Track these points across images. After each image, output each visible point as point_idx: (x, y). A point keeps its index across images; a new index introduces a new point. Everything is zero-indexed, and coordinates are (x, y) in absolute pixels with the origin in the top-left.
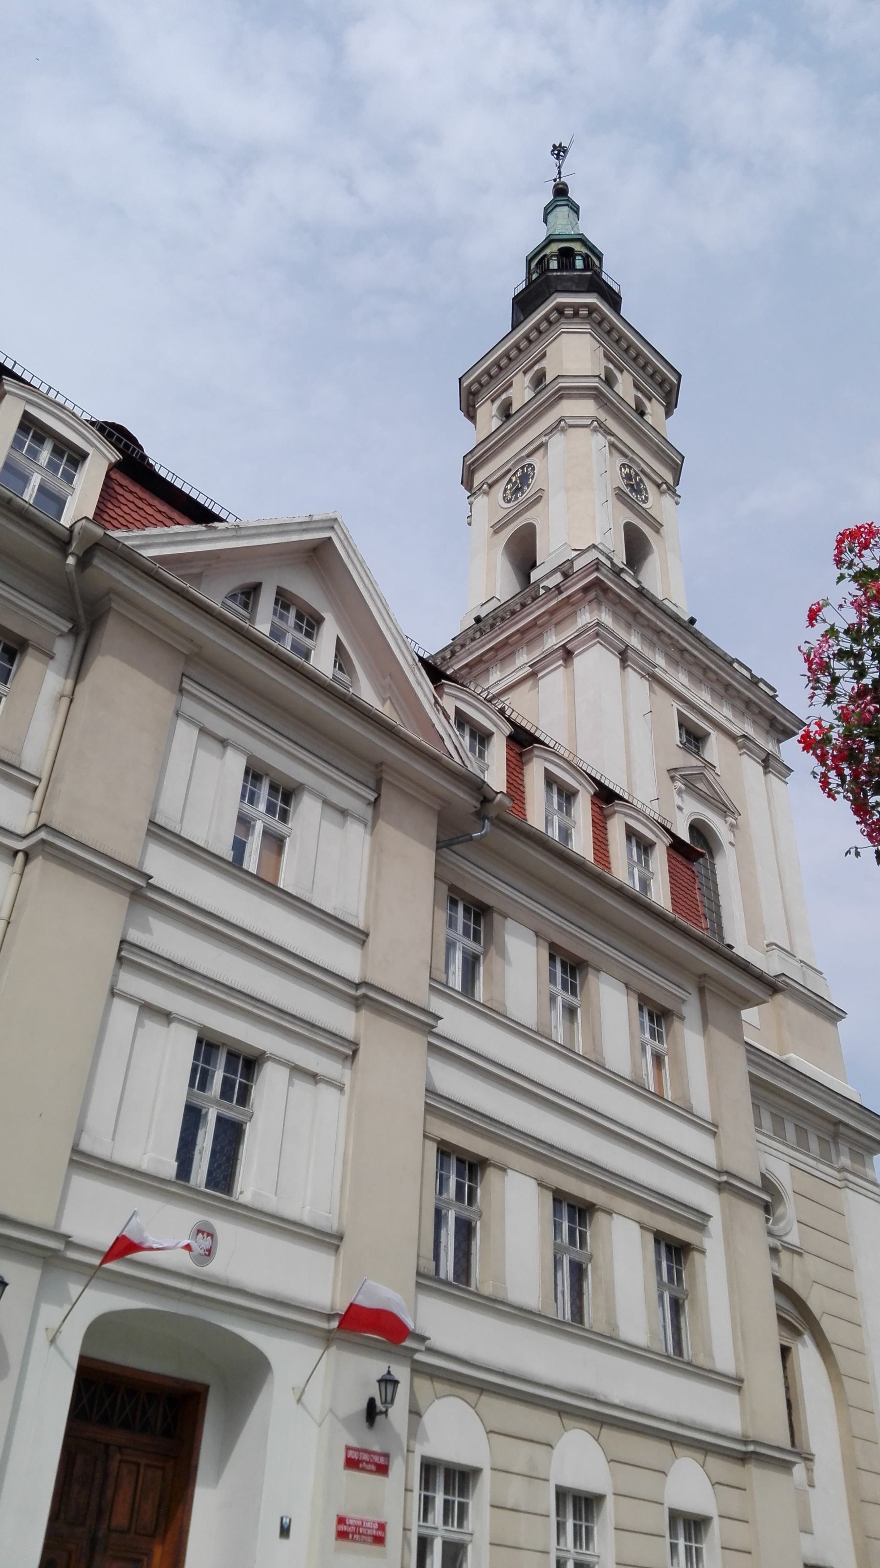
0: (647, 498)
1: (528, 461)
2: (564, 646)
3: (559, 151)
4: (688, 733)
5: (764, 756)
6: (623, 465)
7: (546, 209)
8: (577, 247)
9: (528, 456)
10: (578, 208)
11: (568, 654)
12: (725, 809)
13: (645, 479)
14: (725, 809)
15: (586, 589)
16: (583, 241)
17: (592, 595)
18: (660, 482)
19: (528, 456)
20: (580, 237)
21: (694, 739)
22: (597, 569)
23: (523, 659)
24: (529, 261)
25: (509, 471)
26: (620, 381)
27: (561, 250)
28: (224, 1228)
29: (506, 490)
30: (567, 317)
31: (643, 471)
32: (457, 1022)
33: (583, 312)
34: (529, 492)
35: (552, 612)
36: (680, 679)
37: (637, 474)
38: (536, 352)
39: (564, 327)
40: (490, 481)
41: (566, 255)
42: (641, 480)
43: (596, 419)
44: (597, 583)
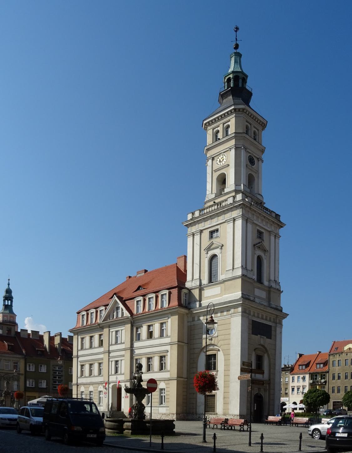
0: (254, 164)
3: (237, 29)
6: (249, 156)
12: (265, 251)
14: (265, 251)
21: (260, 234)
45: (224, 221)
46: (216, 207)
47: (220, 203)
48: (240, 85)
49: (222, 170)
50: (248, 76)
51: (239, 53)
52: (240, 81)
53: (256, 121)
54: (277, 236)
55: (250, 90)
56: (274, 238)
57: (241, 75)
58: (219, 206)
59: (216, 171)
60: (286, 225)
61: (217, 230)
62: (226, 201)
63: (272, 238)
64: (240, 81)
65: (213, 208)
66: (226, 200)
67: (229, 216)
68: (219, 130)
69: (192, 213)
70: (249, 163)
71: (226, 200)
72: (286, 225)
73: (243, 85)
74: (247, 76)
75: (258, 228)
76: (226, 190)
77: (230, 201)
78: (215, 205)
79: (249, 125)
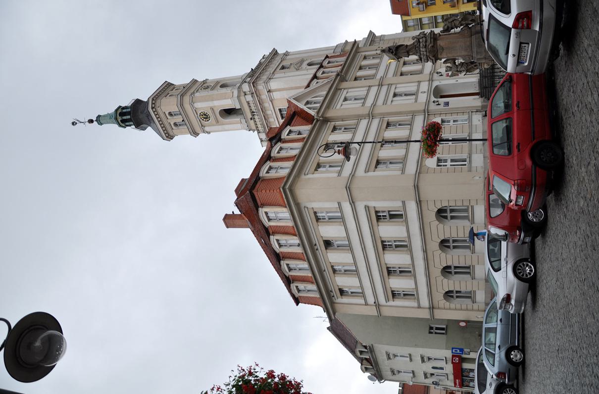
1: (199, 114)
2: (268, 92)
7: (99, 124)
8: (118, 112)
9: (197, 114)
10: (99, 115)
11: (269, 91)
12: (302, 61)
15: (254, 86)
16: (116, 110)
19: (197, 114)
21: (283, 68)
23: (267, 104)
24: (120, 126)
27: (120, 116)
28: (420, 91)
29: (205, 121)
30: (155, 106)
32: (381, 73)
33: (154, 102)
34: (210, 113)
35: (257, 96)
36: (271, 70)
38: (162, 115)
40: (201, 126)
43: (191, 94)
44: (253, 83)
45: (270, 103)
46: (256, 117)
48: (129, 110)
49: (216, 113)
51: (97, 117)
52: (124, 111)
54: (287, 54)
56: (288, 56)
57: (120, 111)
59: (217, 122)
61: (280, 110)
62: (249, 103)
63: (288, 57)
64: (124, 111)
65: (257, 120)
66: (248, 103)
67: (264, 96)
70: (209, 89)
73: (128, 108)
74: (120, 107)
75: (278, 70)
76: (238, 107)
77: (249, 98)
78: (254, 118)
79: (169, 95)
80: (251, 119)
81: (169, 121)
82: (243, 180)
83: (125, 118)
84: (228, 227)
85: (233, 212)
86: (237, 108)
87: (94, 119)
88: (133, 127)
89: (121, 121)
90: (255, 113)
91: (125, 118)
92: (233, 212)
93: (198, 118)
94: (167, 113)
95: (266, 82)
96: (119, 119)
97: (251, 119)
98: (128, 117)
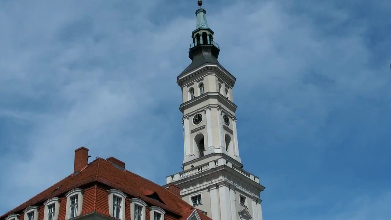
1: (200, 113)
2: (216, 184)
4: (243, 201)
5: (256, 199)
10: (205, 11)
13: (229, 118)
17: (223, 172)
18: (232, 117)
20: (208, 29)
21: (242, 199)
22: (224, 167)
23: (206, 184)
25: (194, 114)
26: (222, 86)
31: (228, 115)
33: (213, 69)
37: (227, 117)
39: (209, 73)
40: (189, 115)
41: (205, 35)
42: (228, 118)
43: (219, 106)
45: (206, 186)
47: (199, 168)
50: (213, 32)
52: (208, 37)
53: (226, 79)
55: (217, 47)
57: (208, 32)
58: (200, 170)
60: (265, 188)
64: (208, 37)
66: (207, 164)
68: (193, 87)
69: (171, 176)
70: (225, 124)
71: (207, 164)
72: (265, 188)
80: (192, 166)
81: (195, 83)
82: (122, 164)
83: (201, 38)
84: (76, 151)
85: (90, 156)
86: (204, 152)
87: (202, 7)
88: (193, 46)
89: (198, 34)
90: (200, 170)
91: (201, 38)
92: (90, 156)
93: (196, 113)
94: (203, 81)
95: (225, 183)
96: (201, 32)
97: (192, 166)
98: (202, 42)
